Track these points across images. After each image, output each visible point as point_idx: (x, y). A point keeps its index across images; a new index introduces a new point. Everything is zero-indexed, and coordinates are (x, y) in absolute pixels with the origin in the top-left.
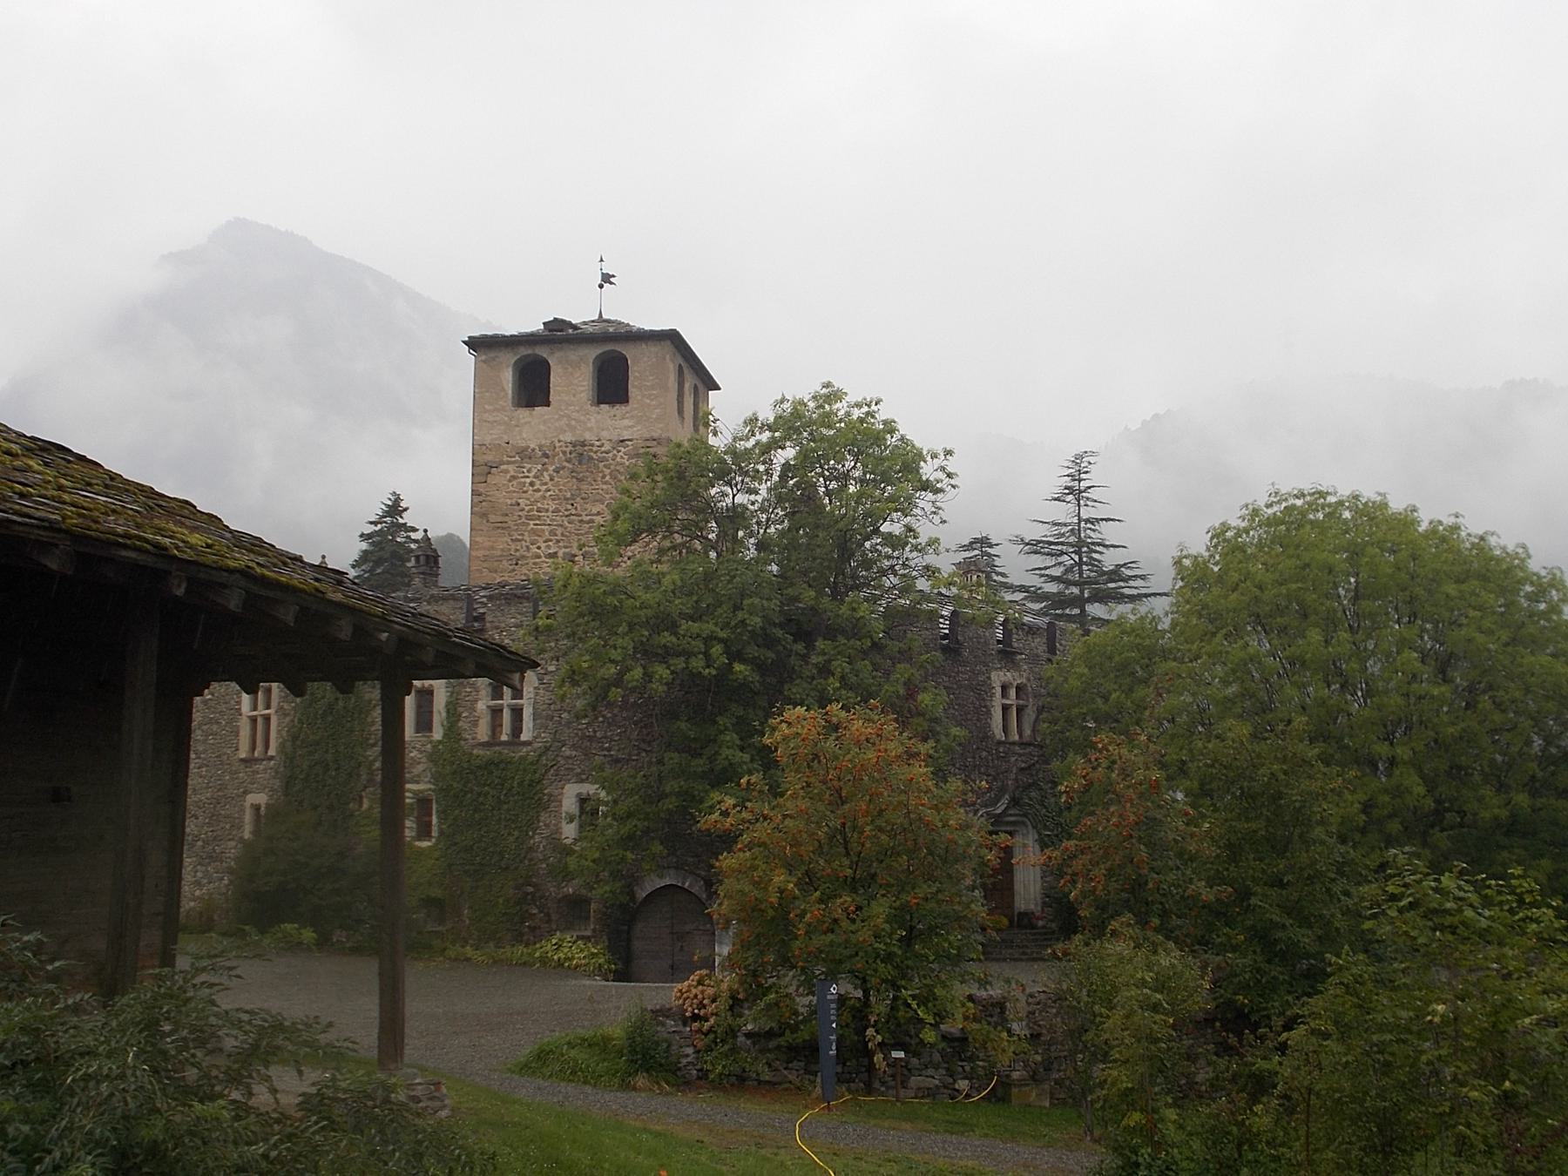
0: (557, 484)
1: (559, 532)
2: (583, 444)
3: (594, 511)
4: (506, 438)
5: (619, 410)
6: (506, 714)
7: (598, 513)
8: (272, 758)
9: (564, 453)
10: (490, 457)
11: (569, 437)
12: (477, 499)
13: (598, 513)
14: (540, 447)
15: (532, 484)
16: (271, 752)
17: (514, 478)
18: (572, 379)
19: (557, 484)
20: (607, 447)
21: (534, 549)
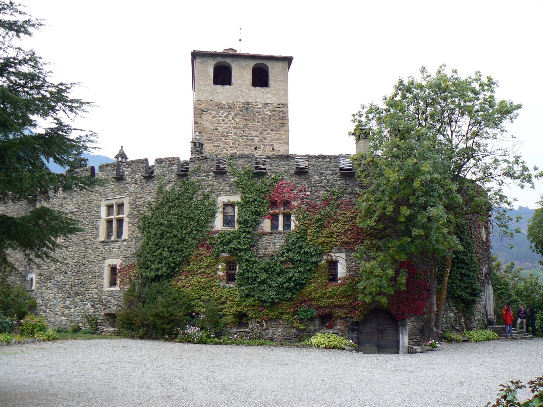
0: (236, 121)
1: (237, 143)
2: (248, 104)
3: (254, 134)
4: (211, 98)
5: (265, 90)
6: (281, 218)
7: (256, 136)
8: (125, 240)
9: (239, 107)
10: (202, 106)
11: (241, 100)
12: (197, 125)
13: (256, 136)
14: (228, 104)
15: (223, 120)
16: (125, 236)
18: (242, 75)
19: (236, 121)
20: (260, 106)
21: (225, 151)
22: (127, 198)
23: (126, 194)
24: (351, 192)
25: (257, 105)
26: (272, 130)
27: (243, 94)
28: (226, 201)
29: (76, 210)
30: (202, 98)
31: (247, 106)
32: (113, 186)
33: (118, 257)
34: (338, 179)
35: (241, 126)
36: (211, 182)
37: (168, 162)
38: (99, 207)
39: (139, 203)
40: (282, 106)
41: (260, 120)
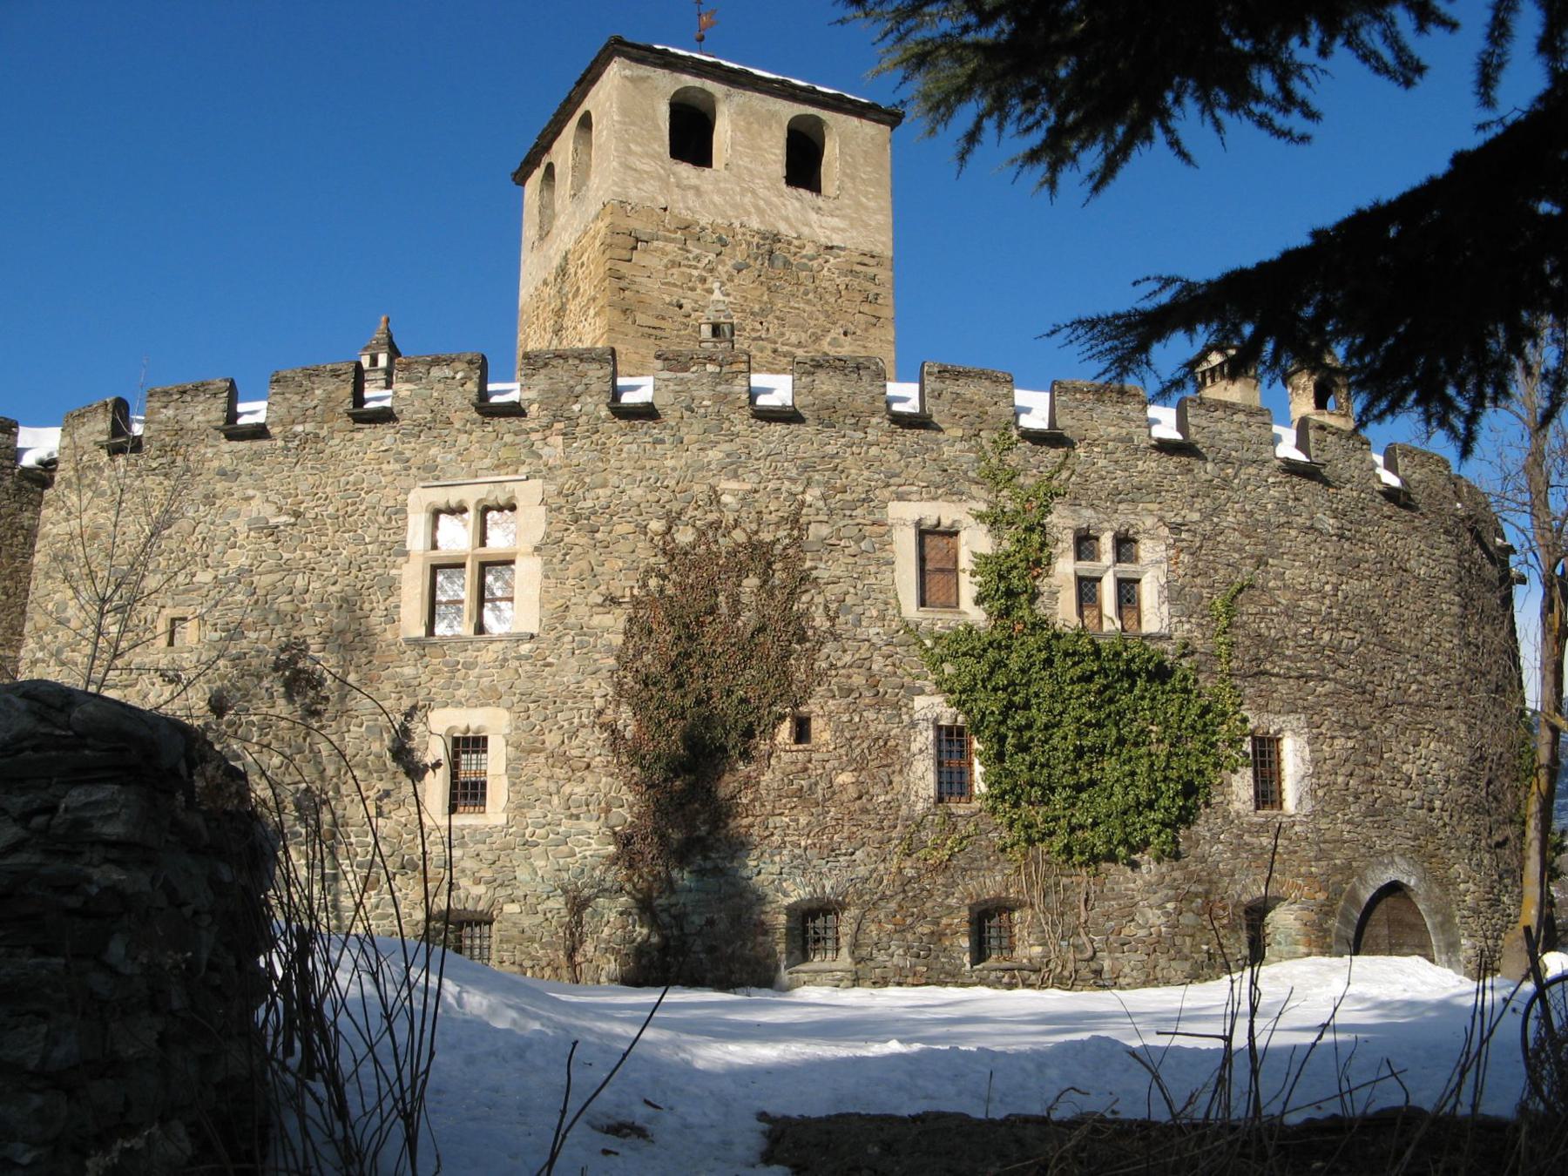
2: (776, 238)
4: (662, 202)
9: (749, 244)
10: (638, 225)
11: (755, 224)
13: (799, 345)
17: (675, 264)
20: (809, 250)
22: (537, 484)
23: (524, 469)
24: (1308, 523)
25: (802, 247)
26: (845, 334)
27: (761, 203)
28: (930, 522)
29: (284, 519)
30: (634, 194)
31: (770, 247)
32: (463, 438)
33: (490, 697)
34: (1271, 480)
35: (756, 308)
36: (874, 451)
37: (710, 368)
38: (402, 511)
39: (589, 503)
40: (871, 262)
41: (811, 296)
